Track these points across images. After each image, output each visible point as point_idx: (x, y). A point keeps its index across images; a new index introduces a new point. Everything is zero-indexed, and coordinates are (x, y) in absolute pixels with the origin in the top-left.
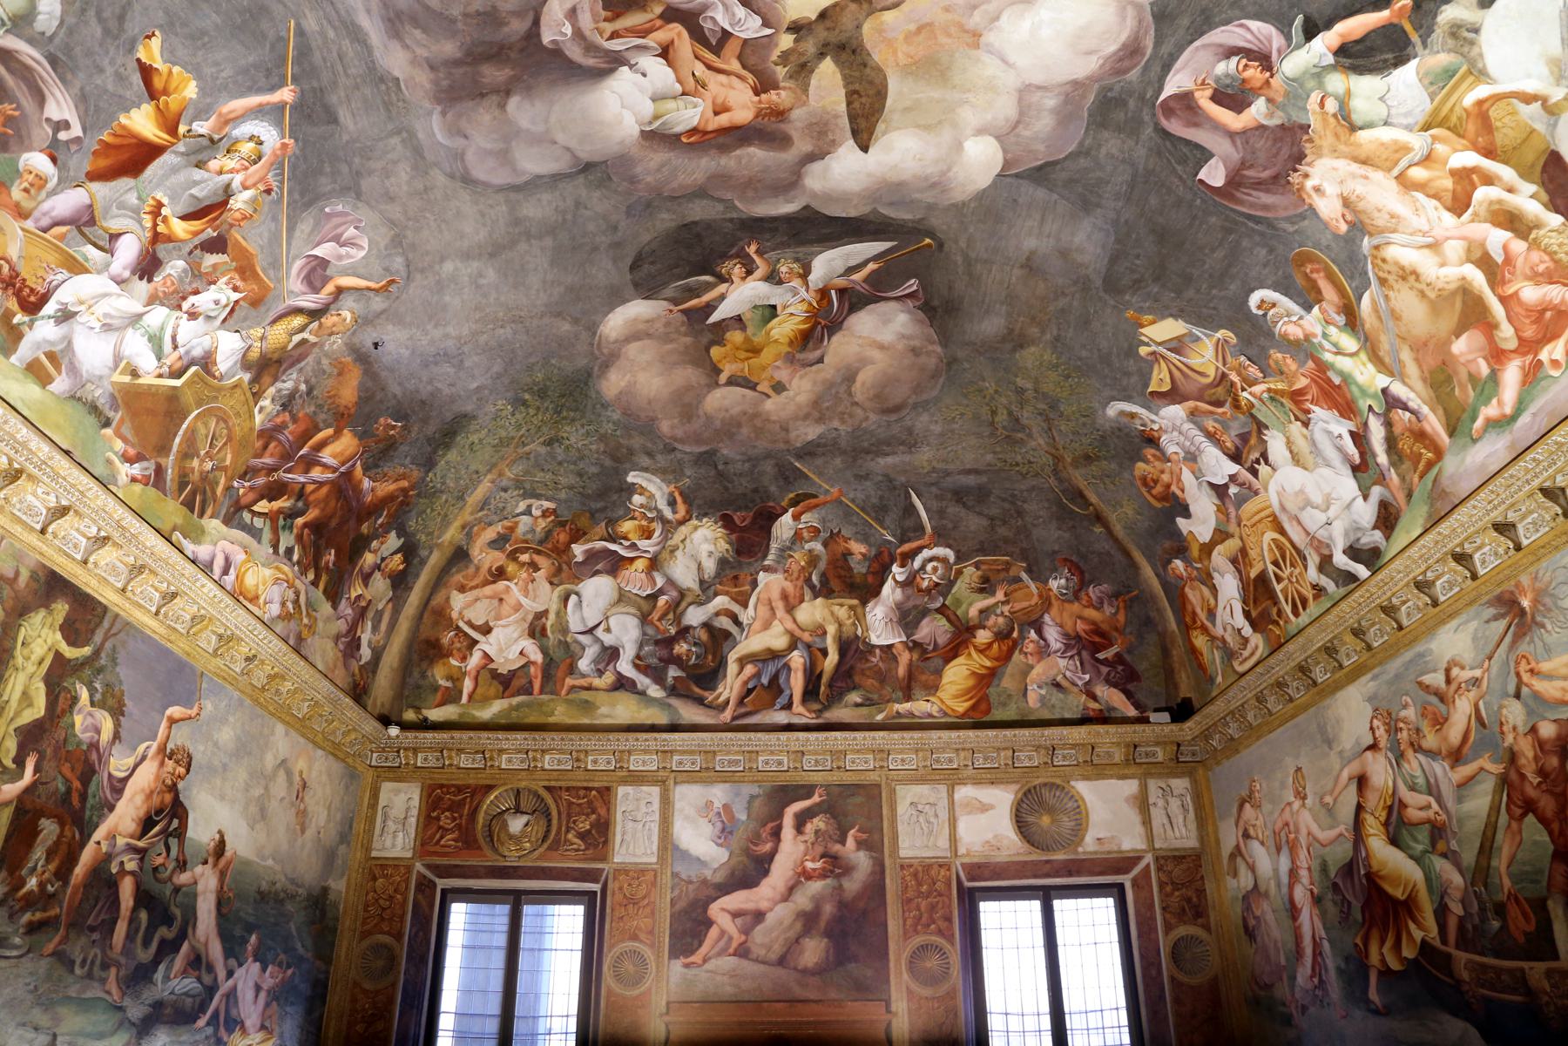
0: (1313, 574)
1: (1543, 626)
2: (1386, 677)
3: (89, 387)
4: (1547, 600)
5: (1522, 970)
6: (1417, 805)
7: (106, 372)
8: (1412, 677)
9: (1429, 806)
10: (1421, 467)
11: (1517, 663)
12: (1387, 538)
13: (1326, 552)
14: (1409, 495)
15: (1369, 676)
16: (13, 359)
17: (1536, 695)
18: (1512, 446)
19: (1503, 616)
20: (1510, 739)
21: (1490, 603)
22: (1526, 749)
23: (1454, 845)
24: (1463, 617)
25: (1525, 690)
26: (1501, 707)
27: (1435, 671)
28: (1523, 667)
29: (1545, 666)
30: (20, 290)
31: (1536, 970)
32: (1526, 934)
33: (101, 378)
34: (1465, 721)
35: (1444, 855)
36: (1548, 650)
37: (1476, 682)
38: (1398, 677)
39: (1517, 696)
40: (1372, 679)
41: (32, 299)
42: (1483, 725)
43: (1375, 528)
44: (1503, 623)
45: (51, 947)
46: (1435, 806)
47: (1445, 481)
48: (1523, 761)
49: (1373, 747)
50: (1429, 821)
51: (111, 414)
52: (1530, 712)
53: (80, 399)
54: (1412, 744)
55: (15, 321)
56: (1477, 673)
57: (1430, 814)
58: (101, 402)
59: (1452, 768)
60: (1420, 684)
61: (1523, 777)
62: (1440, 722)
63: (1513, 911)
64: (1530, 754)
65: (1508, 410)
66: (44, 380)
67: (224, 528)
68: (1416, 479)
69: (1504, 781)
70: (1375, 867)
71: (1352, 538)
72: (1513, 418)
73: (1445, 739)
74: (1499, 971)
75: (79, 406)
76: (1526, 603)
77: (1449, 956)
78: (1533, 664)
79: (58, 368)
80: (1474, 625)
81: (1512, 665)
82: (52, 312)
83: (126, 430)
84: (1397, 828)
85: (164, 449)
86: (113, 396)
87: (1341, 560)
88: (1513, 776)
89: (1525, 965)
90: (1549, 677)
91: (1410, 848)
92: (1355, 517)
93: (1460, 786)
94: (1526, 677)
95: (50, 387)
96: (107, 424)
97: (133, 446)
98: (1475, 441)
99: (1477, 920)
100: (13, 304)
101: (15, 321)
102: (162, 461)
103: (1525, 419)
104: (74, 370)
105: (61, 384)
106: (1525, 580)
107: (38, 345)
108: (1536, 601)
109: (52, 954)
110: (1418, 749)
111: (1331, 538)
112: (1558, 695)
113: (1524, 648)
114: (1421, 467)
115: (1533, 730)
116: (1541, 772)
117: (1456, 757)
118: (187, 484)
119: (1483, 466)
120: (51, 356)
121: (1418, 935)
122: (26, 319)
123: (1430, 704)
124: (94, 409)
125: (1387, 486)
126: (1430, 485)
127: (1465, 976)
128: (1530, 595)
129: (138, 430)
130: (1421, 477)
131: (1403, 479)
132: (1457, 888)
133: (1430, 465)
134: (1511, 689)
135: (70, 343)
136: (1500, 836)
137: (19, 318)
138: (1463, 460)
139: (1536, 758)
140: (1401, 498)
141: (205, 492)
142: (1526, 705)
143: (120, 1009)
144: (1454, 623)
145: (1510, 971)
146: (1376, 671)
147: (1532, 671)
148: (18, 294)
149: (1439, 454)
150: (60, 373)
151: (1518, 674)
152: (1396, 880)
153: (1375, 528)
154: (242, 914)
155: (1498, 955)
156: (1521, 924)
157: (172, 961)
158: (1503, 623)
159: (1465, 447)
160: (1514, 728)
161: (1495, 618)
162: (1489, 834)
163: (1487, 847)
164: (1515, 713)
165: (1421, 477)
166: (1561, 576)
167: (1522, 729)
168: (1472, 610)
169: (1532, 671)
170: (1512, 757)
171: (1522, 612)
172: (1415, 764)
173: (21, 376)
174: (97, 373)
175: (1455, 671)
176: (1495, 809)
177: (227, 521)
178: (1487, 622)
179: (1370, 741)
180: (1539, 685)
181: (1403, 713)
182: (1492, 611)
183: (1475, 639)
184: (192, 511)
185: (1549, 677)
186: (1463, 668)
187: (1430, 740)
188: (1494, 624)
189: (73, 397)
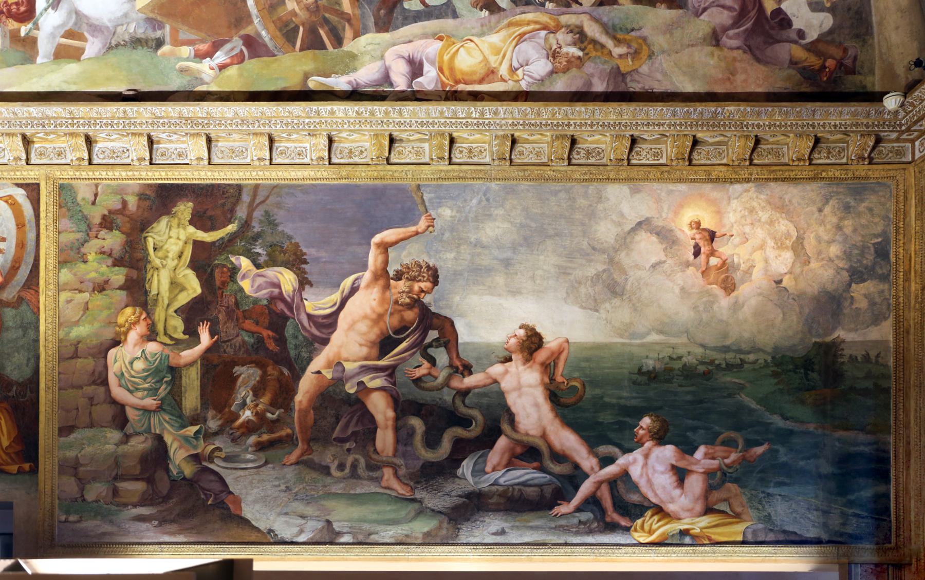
3: (120, 30)
7: (127, 7)
16: (39, 60)
30: (9, 11)
33: (126, 15)
41: (22, 9)
45: (293, 457)
51: (158, 34)
53: (117, 46)
55: (23, 34)
58: (140, 33)
66: (75, 55)
67: (386, 36)
75: (121, 51)
79: (81, 37)
82: (45, 5)
83: (184, 35)
85: (241, 18)
86: (149, 20)
95: (85, 56)
96: (160, 43)
97: (202, 41)
100: (12, 24)
101: (23, 34)
102: (249, 30)
104: (96, 29)
105: (92, 47)
107: (53, 35)
109: (297, 463)
118: (296, 29)
120: (69, 34)
122: (30, 25)
124: (137, 42)
129: (197, 26)
135: (77, 13)
137: (24, 30)
141: (326, 21)
143: (414, 500)
148: (10, 15)
150: (85, 40)
154: (607, 399)
157: (485, 456)
173: (54, 67)
174: (119, 14)
177: (384, 26)
184: (323, 47)
189: (110, 48)
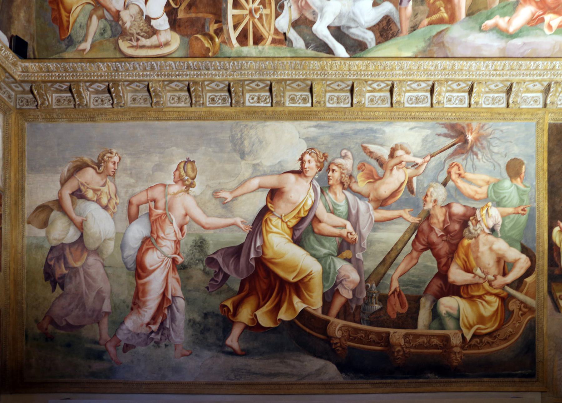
0: (283, 23)
1: (476, 155)
2: (331, 130)
4: (485, 143)
5: (388, 334)
6: (330, 223)
8: (359, 141)
9: (345, 227)
10: (434, 17)
11: (451, 166)
12: (378, 43)
13: (310, 17)
14: (414, 28)
15: (313, 123)
17: (457, 189)
18: (503, 50)
19: (452, 137)
20: (429, 206)
21: (445, 126)
22: (440, 215)
23: (359, 255)
24: (421, 124)
25: (450, 183)
26: (429, 186)
27: (382, 145)
28: (454, 170)
29: (469, 176)
31: (397, 335)
32: (398, 314)
34: (398, 185)
35: (349, 260)
36: (474, 168)
37: (416, 165)
38: (344, 135)
39: (445, 184)
40: (315, 126)
42: (412, 192)
43: (370, 29)
44: (450, 141)
46: (350, 228)
47: (447, 38)
48: (435, 221)
49: (300, 173)
50: (340, 236)
52: (449, 196)
54: (342, 183)
56: (419, 161)
57: (344, 232)
59: (375, 209)
60: (365, 148)
61: (432, 229)
62: (374, 178)
63: (394, 300)
64: (441, 218)
65: (511, 30)
68: (426, 21)
69: (417, 228)
70: (269, 254)
71: (343, 22)
72: (512, 36)
73: (376, 190)
74: (368, 333)
76: (470, 137)
77: (327, 322)
78: (462, 172)
80: (427, 132)
81: (447, 166)
84: (304, 231)
87: (321, 29)
88: (425, 226)
89: (391, 331)
90: (470, 182)
91: (313, 248)
92: (357, 12)
93: (376, 221)
94: (454, 176)
98: (481, 30)
99: (361, 303)
103: (518, 42)
106: (475, 125)
108: (477, 140)
110: (346, 186)
111: (322, 9)
112: (472, 193)
113: (459, 160)
114: (434, 17)
115: (449, 206)
116: (446, 230)
117: (382, 203)
119: (478, 48)
121: (299, 305)
123: (369, 164)
125: (399, 11)
126: (434, 33)
127: (338, 334)
128: (474, 135)
130: (430, 24)
131: (415, 14)
132: (352, 282)
133: (441, 21)
134: (442, 178)
136: (400, 258)
138: (467, 35)
139: (444, 222)
140: (406, 26)
142: (448, 191)
144: (412, 124)
145: (378, 334)
146: (322, 123)
147: (460, 175)
149: (452, 19)
151: (449, 173)
152: (290, 268)
153: (370, 29)
155: (371, 324)
156: (396, 308)
158: (450, 141)
159: (472, 29)
160: (435, 201)
161: (446, 136)
162: (393, 255)
163: (389, 260)
164: (439, 193)
165: (430, 24)
166: (497, 134)
167: (440, 203)
168: (431, 123)
169: (460, 175)
170: (428, 216)
171: (466, 141)
172: (339, 197)
175: (399, 153)
176: (403, 242)
178: (439, 135)
179: (298, 167)
180: (461, 184)
181: (339, 161)
182: (444, 131)
183: (425, 140)
185: (470, 182)
186: (408, 153)
187: (361, 185)
188: (443, 139)
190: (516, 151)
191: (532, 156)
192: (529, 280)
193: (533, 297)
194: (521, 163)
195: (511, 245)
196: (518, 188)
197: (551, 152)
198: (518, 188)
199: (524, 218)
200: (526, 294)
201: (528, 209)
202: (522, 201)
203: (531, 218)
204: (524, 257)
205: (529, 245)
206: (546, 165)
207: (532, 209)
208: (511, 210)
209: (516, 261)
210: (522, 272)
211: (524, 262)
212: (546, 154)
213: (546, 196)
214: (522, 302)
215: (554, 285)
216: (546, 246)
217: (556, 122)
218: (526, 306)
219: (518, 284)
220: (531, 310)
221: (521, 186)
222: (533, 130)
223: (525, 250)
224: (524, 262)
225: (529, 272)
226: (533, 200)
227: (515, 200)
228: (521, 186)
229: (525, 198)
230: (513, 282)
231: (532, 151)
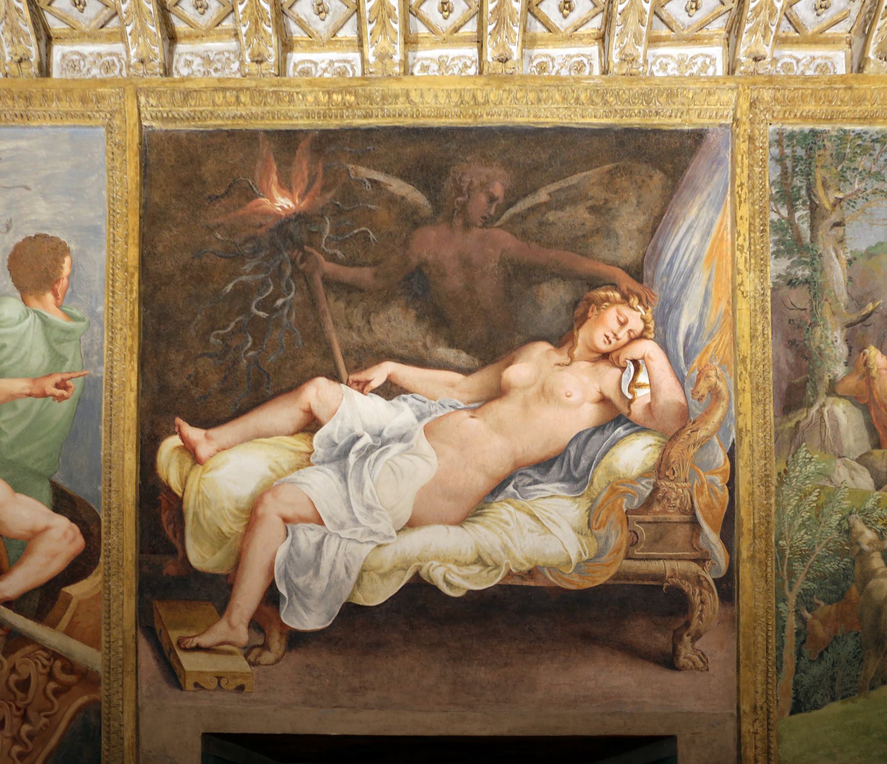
190: (41, 215)
191: (96, 230)
192: (77, 590)
193: (94, 643)
194: (59, 249)
195: (17, 488)
196: (45, 323)
197: (151, 219)
198: (45, 323)
199: (61, 411)
200: (69, 632)
201: (76, 385)
202: (58, 359)
203: (87, 409)
204: (61, 523)
205: (80, 489)
206: (133, 253)
207: (92, 385)
208: (19, 385)
209: (35, 535)
210: (56, 566)
211: (60, 539)
212: (134, 221)
213: (134, 343)
214: (55, 655)
215: (161, 609)
216: (130, 492)
217: (171, 127)
218: (70, 666)
219: (44, 600)
220: (87, 678)
221: (57, 317)
222: (99, 151)
223: (63, 502)
224: (60, 539)
225: (78, 568)
226: (95, 358)
227: (37, 355)
228: (57, 317)
229: (69, 350)
230: (26, 596)
231: (94, 214)
